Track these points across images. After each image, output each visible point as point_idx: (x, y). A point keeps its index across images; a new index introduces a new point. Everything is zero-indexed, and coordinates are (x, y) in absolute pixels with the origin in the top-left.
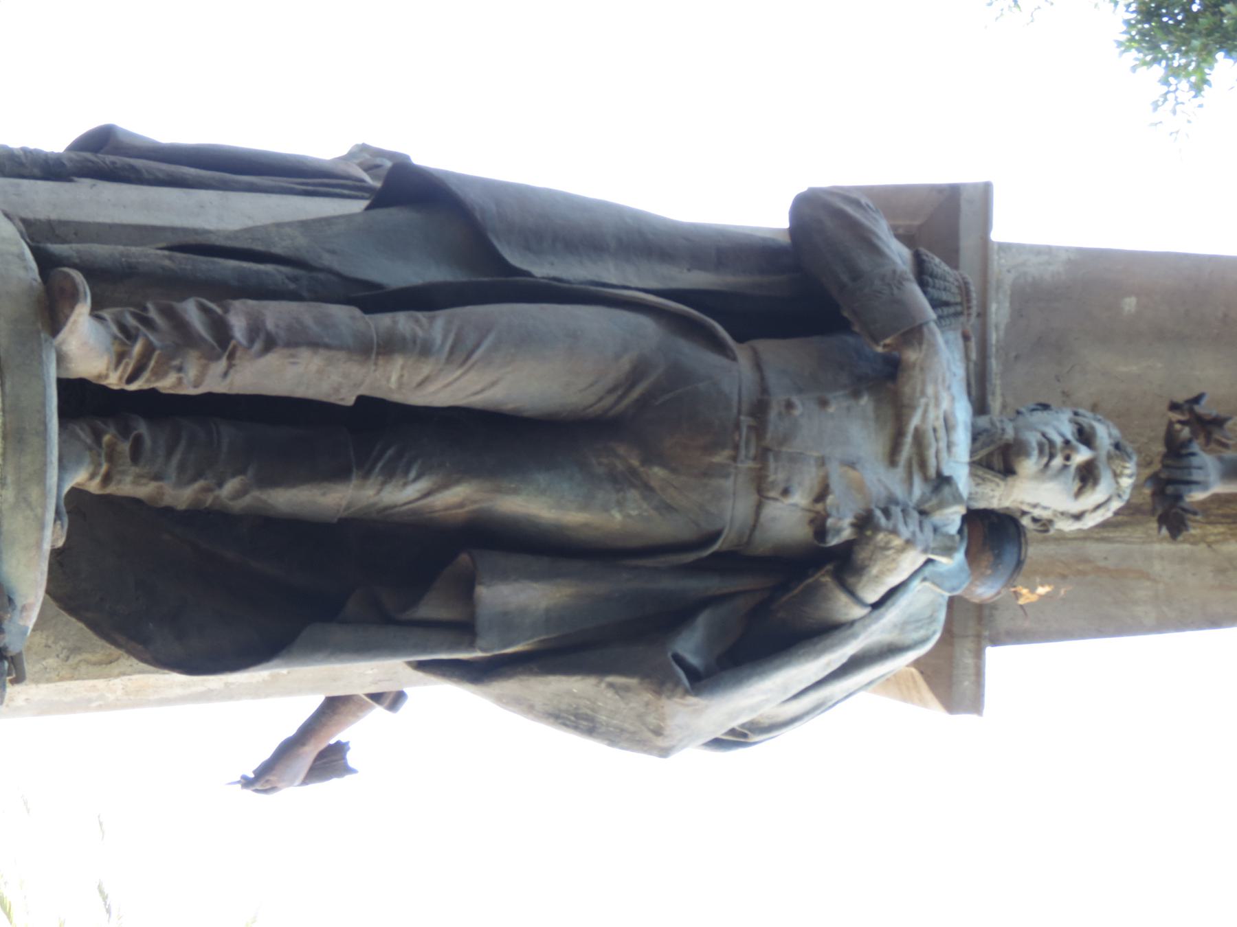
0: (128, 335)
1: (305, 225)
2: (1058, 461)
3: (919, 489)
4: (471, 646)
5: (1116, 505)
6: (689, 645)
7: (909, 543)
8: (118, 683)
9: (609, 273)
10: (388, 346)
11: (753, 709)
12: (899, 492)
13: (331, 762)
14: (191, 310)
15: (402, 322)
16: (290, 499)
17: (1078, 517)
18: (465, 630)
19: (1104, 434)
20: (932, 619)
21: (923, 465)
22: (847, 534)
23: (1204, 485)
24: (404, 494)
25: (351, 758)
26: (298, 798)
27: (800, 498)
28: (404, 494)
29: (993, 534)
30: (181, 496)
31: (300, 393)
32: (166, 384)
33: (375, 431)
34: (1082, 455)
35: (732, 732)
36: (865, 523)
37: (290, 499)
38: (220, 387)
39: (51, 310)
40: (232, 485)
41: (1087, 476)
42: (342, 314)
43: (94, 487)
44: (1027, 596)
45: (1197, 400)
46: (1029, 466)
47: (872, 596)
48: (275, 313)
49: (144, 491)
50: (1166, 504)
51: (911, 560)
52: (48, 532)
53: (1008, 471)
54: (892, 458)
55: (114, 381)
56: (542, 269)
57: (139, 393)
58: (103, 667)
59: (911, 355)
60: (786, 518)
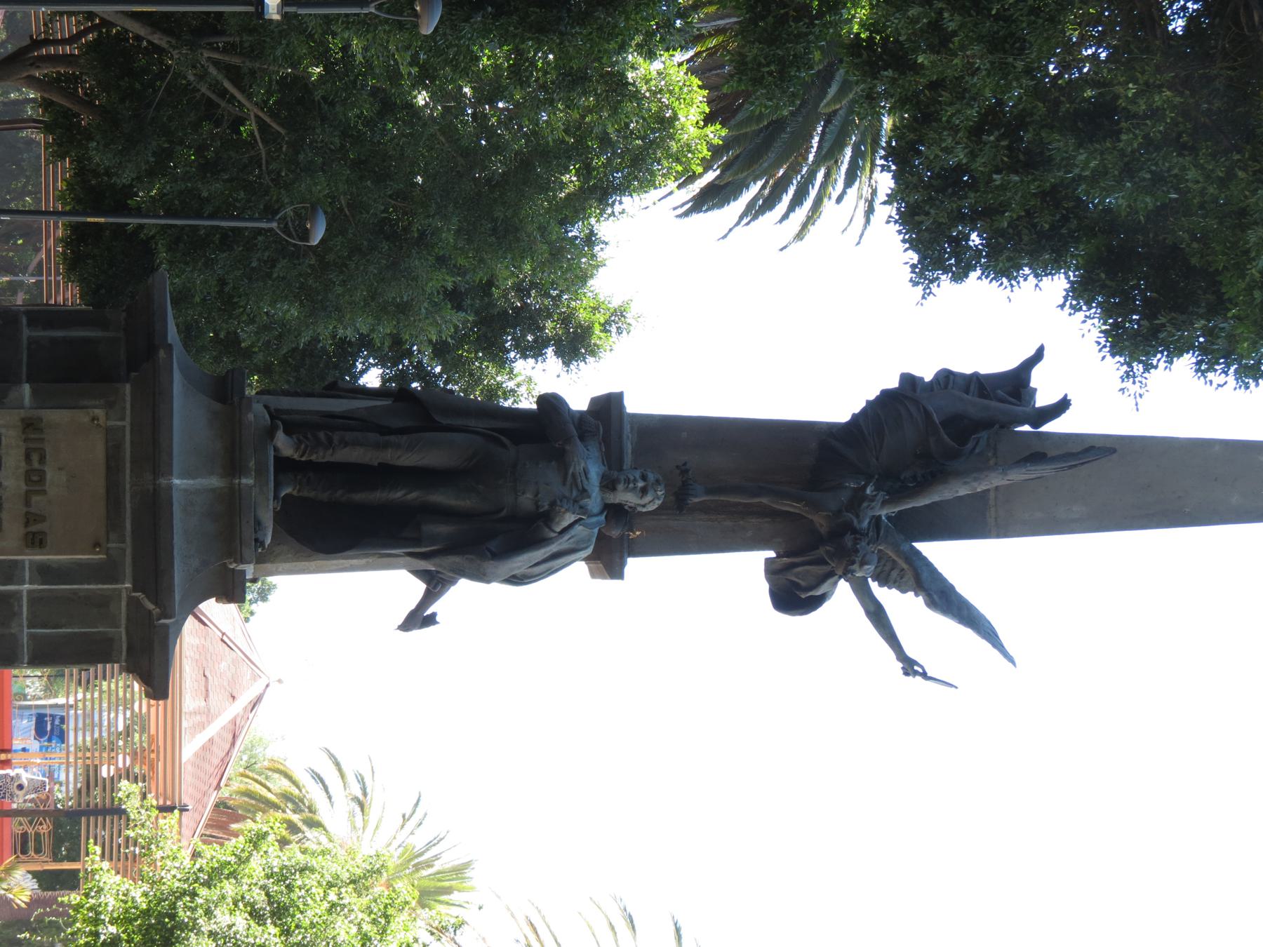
0: (300, 442)
1: (367, 409)
2: (631, 485)
3: (575, 493)
4: (420, 546)
5: (658, 503)
6: (493, 545)
7: (567, 510)
8: (313, 564)
9: (472, 423)
10: (385, 446)
11: (519, 568)
12: (567, 494)
13: (430, 620)
14: (322, 435)
15: (392, 438)
16: (359, 497)
17: (644, 506)
18: (417, 542)
19: (651, 477)
20: (589, 540)
21: (577, 486)
22: (546, 507)
23: (696, 496)
24: (398, 495)
25: (438, 619)
26: (417, 634)
27: (529, 495)
28: (398, 495)
29: (616, 512)
30: (324, 496)
31: (359, 461)
32: (313, 458)
33: (388, 474)
34: (641, 484)
35: (514, 576)
36: (553, 504)
37: (359, 497)
38: (332, 459)
39: (271, 432)
40: (339, 493)
41: (644, 491)
42: (373, 436)
43: (295, 493)
44: (632, 535)
45: (685, 464)
46: (620, 487)
47: (558, 530)
48: (349, 436)
49: (312, 494)
50: (679, 501)
51: (569, 518)
52: (271, 502)
53: (614, 489)
54: (564, 484)
55: (296, 457)
56: (445, 421)
57: (306, 462)
58: (308, 558)
59: (568, 447)
60: (526, 501)
